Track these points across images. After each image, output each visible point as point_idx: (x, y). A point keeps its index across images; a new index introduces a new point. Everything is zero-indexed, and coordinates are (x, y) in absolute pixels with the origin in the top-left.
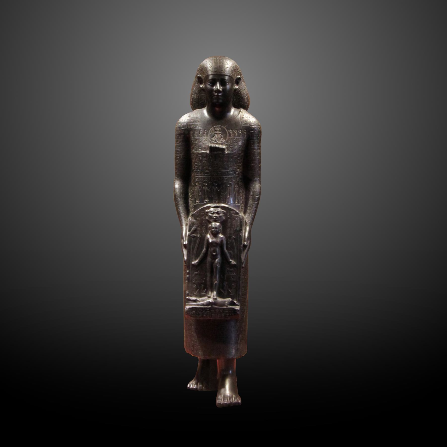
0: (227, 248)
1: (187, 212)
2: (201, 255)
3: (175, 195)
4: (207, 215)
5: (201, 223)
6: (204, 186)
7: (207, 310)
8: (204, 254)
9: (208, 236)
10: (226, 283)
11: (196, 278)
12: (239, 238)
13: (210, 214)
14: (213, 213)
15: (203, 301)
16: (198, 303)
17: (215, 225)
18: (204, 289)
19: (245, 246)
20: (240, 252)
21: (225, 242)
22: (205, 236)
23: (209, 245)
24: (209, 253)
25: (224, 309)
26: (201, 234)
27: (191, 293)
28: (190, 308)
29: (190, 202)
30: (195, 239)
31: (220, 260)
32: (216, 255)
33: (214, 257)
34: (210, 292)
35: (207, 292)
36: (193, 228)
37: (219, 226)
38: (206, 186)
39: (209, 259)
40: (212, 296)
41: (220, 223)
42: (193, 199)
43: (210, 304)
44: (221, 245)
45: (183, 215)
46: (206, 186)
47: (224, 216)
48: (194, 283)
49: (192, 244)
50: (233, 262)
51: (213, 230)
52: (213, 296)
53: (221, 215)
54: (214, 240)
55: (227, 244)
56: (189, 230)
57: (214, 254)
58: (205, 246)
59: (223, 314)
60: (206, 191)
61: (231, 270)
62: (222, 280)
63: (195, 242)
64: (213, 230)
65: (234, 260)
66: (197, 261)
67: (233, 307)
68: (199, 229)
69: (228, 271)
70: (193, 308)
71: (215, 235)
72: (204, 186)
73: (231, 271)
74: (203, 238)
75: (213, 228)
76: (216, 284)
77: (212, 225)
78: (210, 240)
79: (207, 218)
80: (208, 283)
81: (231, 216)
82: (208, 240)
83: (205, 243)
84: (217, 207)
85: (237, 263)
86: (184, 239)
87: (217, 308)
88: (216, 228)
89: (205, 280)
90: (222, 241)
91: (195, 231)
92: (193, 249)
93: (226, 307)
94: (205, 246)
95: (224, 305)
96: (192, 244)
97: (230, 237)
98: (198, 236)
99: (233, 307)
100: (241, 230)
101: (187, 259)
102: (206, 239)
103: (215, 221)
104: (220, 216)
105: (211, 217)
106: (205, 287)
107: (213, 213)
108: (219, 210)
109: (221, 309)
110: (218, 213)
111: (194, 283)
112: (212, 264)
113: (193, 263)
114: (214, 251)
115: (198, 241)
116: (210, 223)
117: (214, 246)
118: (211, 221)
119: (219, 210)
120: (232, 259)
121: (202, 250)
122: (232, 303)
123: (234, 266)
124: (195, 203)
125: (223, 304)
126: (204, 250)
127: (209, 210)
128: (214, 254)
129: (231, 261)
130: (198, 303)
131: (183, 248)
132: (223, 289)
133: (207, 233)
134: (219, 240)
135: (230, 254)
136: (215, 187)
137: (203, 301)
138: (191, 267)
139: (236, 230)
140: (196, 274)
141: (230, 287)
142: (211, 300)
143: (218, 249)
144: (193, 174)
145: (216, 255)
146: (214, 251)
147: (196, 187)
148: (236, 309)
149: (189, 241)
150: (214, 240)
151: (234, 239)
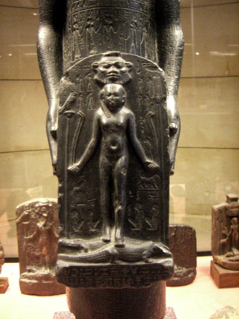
0: (139, 137)
1: (59, 71)
2: (87, 151)
3: (39, 50)
4: (96, 72)
5: (84, 88)
6: (88, 26)
7: (102, 272)
8: (91, 148)
9: (100, 112)
10: (141, 206)
11: (78, 199)
12: (163, 117)
13: (101, 69)
14: (108, 66)
15: (93, 248)
16: (81, 254)
17: (113, 88)
18: (94, 221)
19: (173, 131)
20: (166, 144)
21: (133, 121)
22: (92, 113)
23: (102, 129)
24: (103, 147)
25: (139, 266)
26: (85, 109)
27: (69, 230)
28: (65, 269)
29: (65, 60)
30: (72, 119)
31: (126, 160)
32: (119, 150)
33: (113, 156)
34: (108, 230)
35: (99, 227)
36: (68, 99)
37: (121, 90)
38: (92, 26)
39: (103, 159)
40: (113, 239)
41: (124, 85)
42: (70, 54)
43: (108, 257)
44: (126, 129)
45: (51, 80)
46: (92, 26)
47: (130, 71)
48: (75, 210)
49: (67, 130)
50: (153, 164)
51: (109, 98)
52: (116, 239)
53: (124, 69)
54: (113, 118)
55: (139, 128)
56: (61, 103)
57: (114, 148)
58: (93, 134)
59: (138, 279)
60: (91, 35)
61: (148, 179)
62: (130, 202)
63: (72, 127)
64: (109, 98)
65: (154, 159)
66: (78, 164)
67: (160, 261)
68: (80, 99)
69: (143, 182)
70: (71, 268)
71: (113, 108)
72: (88, 26)
73: (148, 183)
74: (87, 119)
75: (110, 94)
76: (119, 211)
77: (106, 89)
78: (104, 120)
79: (96, 77)
80: (104, 211)
81: (144, 72)
82: (99, 120)
83: (94, 125)
84: (117, 55)
85: (161, 165)
86: (53, 121)
87: (123, 267)
88: (115, 94)
89: (97, 203)
90: (128, 121)
91: (73, 103)
92: (70, 138)
93: (144, 263)
94: (93, 134)
95: (140, 259)
96: (67, 130)
97: (143, 114)
98: (80, 112)
99: (160, 261)
100: (165, 99)
101: (58, 160)
102: (95, 118)
103: (113, 80)
104: (122, 72)
105: (104, 74)
106: (97, 218)
107: (108, 66)
108: (120, 59)
109: (134, 267)
110: (117, 65)
111: (75, 210)
112: (110, 170)
113: (70, 168)
114: (114, 143)
115: (79, 123)
116: (102, 85)
117: (114, 131)
118: (105, 81)
119: (120, 59)
120: (149, 156)
121: (87, 142)
122: (158, 253)
123: (156, 171)
124: (73, 59)
125: (138, 256)
126: (92, 141)
127: (99, 62)
128: (114, 148)
129: (148, 160)
130: (81, 254)
131: (51, 137)
132: (133, 218)
133: (96, 106)
134: (122, 120)
135: (146, 147)
136: (108, 27)
137: (93, 248)
138: (66, 176)
139: (155, 99)
140: (77, 191)
141: (148, 215)
142: (110, 248)
143: (120, 139)
144: (70, 13)
145: (119, 150)
146: (114, 143)
147: (74, 33)
148: (167, 265)
149: (62, 125)
150: (113, 118)
151: (153, 116)
